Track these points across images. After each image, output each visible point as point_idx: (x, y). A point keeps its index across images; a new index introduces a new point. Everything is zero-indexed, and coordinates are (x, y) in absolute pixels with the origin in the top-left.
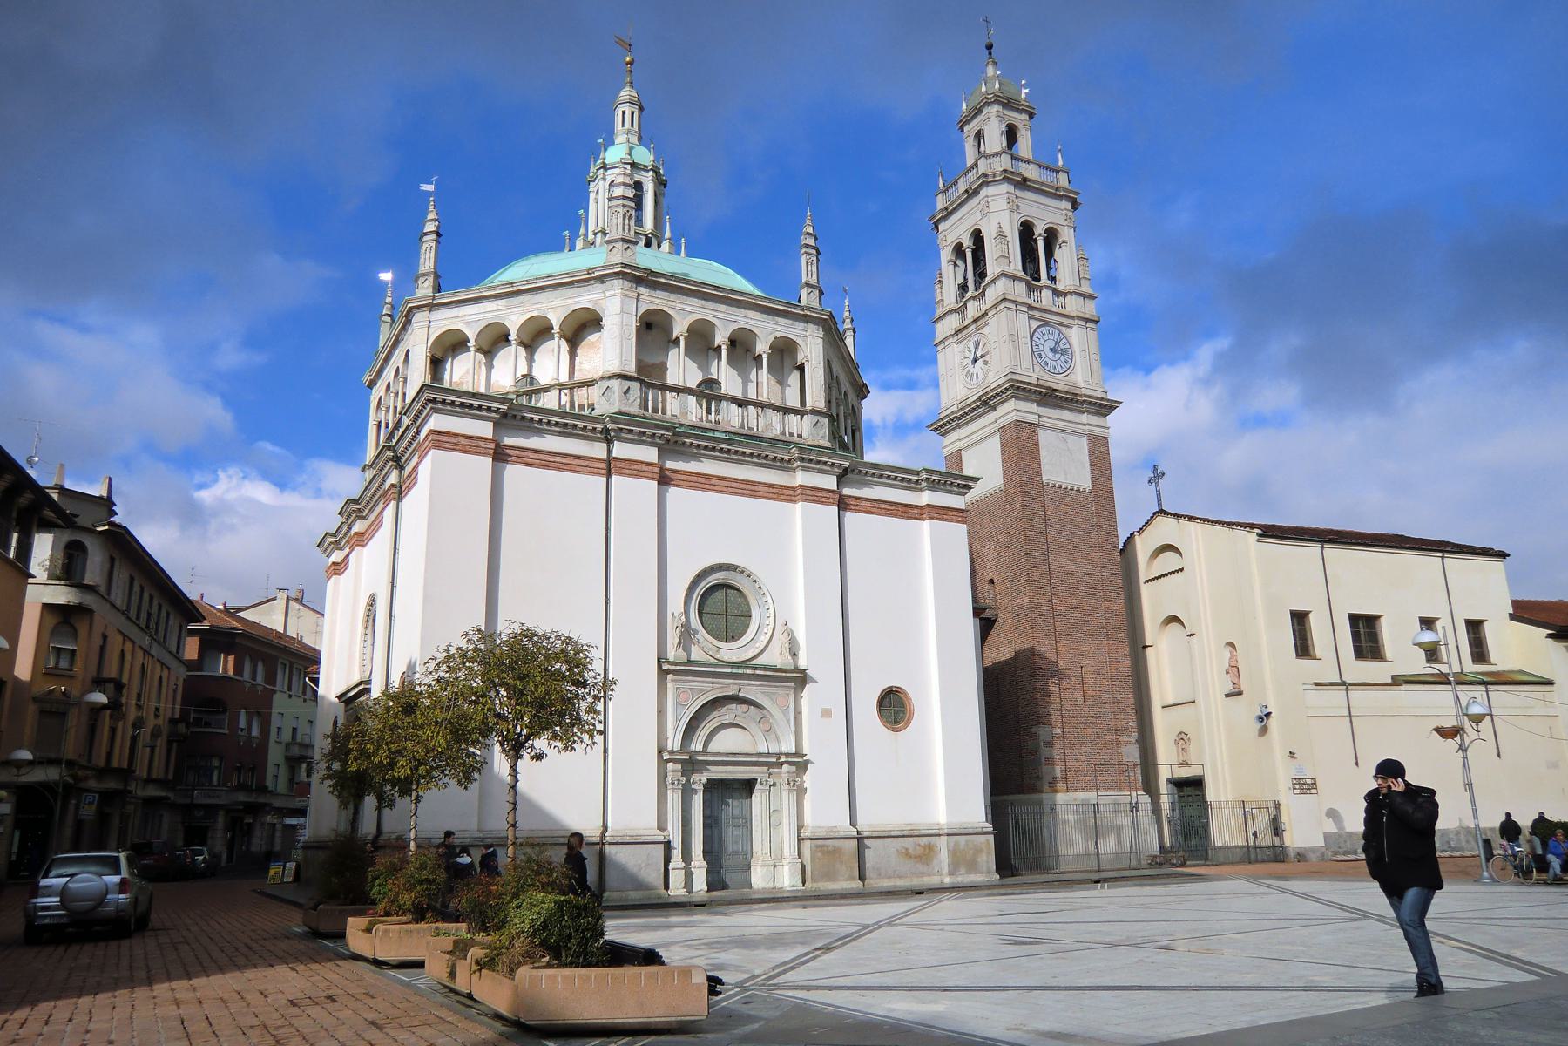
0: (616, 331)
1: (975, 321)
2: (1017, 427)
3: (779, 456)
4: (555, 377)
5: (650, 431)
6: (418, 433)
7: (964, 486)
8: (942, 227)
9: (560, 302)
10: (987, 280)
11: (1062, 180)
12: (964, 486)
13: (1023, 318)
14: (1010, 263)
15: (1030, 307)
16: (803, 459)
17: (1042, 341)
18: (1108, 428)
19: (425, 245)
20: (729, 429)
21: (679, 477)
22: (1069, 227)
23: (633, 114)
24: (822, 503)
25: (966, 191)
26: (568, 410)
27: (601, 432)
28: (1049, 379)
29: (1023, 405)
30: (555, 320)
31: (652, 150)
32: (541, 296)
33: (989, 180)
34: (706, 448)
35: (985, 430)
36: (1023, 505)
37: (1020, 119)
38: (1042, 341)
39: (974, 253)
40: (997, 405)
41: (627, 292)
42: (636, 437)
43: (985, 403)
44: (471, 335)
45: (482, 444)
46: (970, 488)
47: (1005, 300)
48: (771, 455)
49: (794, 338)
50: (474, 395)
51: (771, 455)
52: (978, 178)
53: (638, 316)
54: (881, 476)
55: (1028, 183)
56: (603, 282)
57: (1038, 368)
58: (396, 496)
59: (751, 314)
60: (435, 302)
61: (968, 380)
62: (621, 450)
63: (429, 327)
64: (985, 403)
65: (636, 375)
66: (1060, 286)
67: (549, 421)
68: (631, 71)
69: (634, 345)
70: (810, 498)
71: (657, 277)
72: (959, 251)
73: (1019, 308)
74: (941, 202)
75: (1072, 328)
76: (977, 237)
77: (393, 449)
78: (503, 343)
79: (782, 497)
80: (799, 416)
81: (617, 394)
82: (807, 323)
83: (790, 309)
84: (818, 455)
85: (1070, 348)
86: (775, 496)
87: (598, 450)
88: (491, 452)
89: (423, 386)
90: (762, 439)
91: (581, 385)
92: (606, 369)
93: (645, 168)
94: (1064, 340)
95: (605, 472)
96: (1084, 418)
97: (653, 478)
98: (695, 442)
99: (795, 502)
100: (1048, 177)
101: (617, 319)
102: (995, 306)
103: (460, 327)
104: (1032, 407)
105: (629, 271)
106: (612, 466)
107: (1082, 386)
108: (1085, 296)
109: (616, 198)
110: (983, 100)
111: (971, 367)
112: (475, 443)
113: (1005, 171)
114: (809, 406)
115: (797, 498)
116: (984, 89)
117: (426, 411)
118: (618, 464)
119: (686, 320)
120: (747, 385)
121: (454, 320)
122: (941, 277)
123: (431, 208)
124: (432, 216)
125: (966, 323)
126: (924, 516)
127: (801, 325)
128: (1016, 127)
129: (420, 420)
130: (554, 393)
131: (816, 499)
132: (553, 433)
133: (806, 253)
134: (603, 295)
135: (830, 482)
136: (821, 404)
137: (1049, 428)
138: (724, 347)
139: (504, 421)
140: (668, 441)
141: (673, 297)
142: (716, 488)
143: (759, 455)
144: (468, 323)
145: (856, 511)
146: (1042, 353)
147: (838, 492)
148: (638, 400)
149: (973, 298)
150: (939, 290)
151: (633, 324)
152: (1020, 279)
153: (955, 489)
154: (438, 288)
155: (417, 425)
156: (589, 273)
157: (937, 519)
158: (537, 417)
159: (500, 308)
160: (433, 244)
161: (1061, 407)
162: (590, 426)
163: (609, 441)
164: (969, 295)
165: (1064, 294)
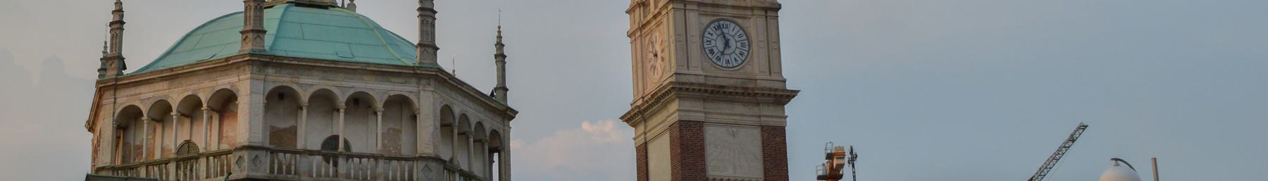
1: (655, 17)
2: (681, 125)
9: (207, 84)
13: (693, 17)
18: (787, 117)
28: (719, 74)
29: (688, 105)
30: (204, 97)
32: (195, 79)
35: (662, 125)
44: (145, 110)
49: (407, 94)
53: (266, 94)
59: (365, 78)
60: (118, 83)
63: (115, 102)
73: (688, 7)
75: (750, 18)
81: (246, 161)
83: (401, 71)
102: (665, 6)
103: (137, 103)
104: (698, 106)
105: (256, 59)
107: (758, 77)
121: (132, 97)
144: (142, 101)
146: (716, 51)
151: (260, 100)
159: (165, 87)
161: (732, 101)
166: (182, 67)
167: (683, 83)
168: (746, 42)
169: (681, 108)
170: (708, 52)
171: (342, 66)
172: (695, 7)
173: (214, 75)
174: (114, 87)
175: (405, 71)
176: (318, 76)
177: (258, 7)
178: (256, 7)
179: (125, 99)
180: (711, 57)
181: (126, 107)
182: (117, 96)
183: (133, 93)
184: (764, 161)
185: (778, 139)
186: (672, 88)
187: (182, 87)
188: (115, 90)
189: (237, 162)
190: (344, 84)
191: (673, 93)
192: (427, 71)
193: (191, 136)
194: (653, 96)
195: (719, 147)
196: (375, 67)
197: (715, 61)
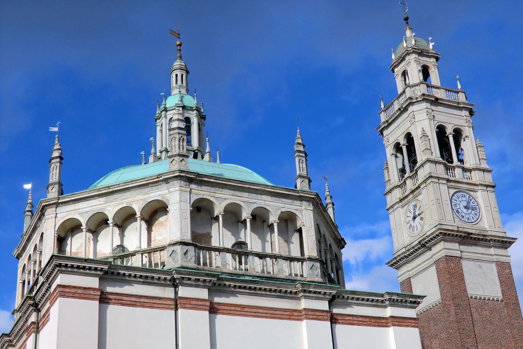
0: (177, 213)
1: (412, 192)
2: (446, 260)
3: (289, 290)
4: (139, 246)
5: (202, 278)
6: (50, 287)
7: (414, 302)
8: (385, 133)
9: (140, 197)
10: (418, 165)
11: (461, 97)
12: (414, 302)
13: (444, 188)
14: (432, 153)
15: (448, 181)
16: (305, 291)
17: (458, 202)
19: (53, 165)
20: (255, 274)
21: (223, 307)
22: (469, 127)
23: (182, 76)
24: (320, 320)
25: (399, 109)
26: (148, 267)
27: (170, 281)
28: (465, 227)
30: (137, 208)
31: (195, 97)
33: (414, 101)
34: (240, 287)
35: (426, 263)
36: (456, 313)
37: (431, 62)
38: (458, 202)
39: (408, 148)
40: (432, 246)
41: (183, 188)
42: (193, 283)
43: (423, 246)
45: (92, 292)
46: (419, 303)
47: (431, 177)
48: (284, 290)
49: (294, 211)
50: (86, 260)
51: (284, 290)
52: (407, 100)
53: (191, 203)
54: (358, 299)
55: (439, 101)
56: (168, 183)
57: (457, 220)
58: (35, 330)
59: (265, 197)
60: (59, 201)
61: (411, 231)
62: (184, 292)
63: (56, 217)
64: (423, 246)
65: (191, 242)
66: (467, 165)
67: (136, 275)
68: (180, 50)
69: (189, 222)
70: (312, 317)
71: (202, 177)
72: (398, 148)
73: (441, 181)
74: (383, 117)
75: (477, 192)
76: (409, 137)
77: (33, 298)
78: (104, 225)
79: (293, 317)
80: (300, 263)
82: (302, 201)
83: (290, 193)
84: (314, 288)
85: (478, 205)
86: (288, 317)
87: (168, 293)
88: (98, 297)
89: (53, 256)
90: (277, 279)
91: (155, 250)
92: (172, 239)
93: (191, 109)
94: (473, 200)
95: (173, 307)
96: (492, 251)
97: (205, 310)
98: (232, 284)
99: (301, 320)
100: (452, 97)
101: (177, 206)
102: (425, 181)
104: (456, 246)
105: (184, 175)
106: (178, 303)
108: (484, 170)
109: (174, 129)
110: (405, 52)
111: (412, 222)
112: (87, 292)
113: (423, 95)
114: (307, 254)
115: (302, 318)
116: (405, 45)
117: (55, 273)
118: (183, 301)
119: (222, 204)
120: (265, 244)
121: (72, 212)
122: (387, 165)
123: (56, 142)
124: (57, 147)
125: (406, 194)
126: (389, 324)
127: (298, 203)
128: (428, 67)
129: (51, 279)
130: (139, 256)
131: (315, 317)
132: (138, 283)
133: (298, 156)
134: (168, 191)
135: (324, 305)
136: (314, 254)
137: (468, 259)
138: (248, 220)
139: (106, 276)
140: (214, 284)
141: (213, 190)
142: (248, 314)
143: (275, 290)
144: (81, 214)
145: (343, 323)
146: (459, 210)
147: (330, 312)
148: (194, 258)
149: (410, 177)
150: (387, 174)
151: (188, 209)
152: (440, 163)
153: (409, 304)
154: (61, 193)
155: (49, 282)
156: (158, 178)
157: (398, 326)
158: (127, 273)
159: (102, 203)
160: (58, 164)
161: (476, 245)
162: (163, 277)
163: (175, 286)
164: (406, 175)
165: (470, 171)
166: (118, 185)
167: (447, 230)
168: (478, 208)
169: (445, 247)
170: (455, 212)
171: (248, 186)
172: (445, 182)
173: (146, 190)
174: (55, 206)
175: (293, 194)
176: (230, 193)
177: (182, 138)
178: (180, 138)
179: (66, 214)
180: (458, 215)
181: (65, 221)
182: (58, 212)
183: (72, 209)
184: (501, 286)
185: (507, 271)
186: (441, 233)
187: (117, 201)
188: (56, 207)
189: (170, 255)
190: (250, 201)
191: (439, 238)
192: (307, 194)
193: (122, 240)
194: (420, 243)
195: (472, 275)
196: (271, 189)
197: (461, 218)
